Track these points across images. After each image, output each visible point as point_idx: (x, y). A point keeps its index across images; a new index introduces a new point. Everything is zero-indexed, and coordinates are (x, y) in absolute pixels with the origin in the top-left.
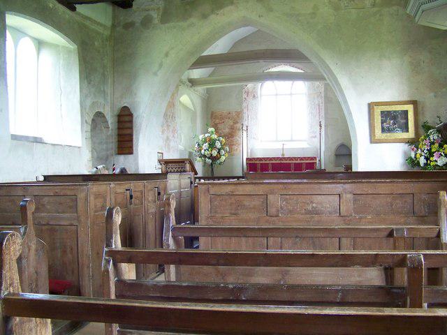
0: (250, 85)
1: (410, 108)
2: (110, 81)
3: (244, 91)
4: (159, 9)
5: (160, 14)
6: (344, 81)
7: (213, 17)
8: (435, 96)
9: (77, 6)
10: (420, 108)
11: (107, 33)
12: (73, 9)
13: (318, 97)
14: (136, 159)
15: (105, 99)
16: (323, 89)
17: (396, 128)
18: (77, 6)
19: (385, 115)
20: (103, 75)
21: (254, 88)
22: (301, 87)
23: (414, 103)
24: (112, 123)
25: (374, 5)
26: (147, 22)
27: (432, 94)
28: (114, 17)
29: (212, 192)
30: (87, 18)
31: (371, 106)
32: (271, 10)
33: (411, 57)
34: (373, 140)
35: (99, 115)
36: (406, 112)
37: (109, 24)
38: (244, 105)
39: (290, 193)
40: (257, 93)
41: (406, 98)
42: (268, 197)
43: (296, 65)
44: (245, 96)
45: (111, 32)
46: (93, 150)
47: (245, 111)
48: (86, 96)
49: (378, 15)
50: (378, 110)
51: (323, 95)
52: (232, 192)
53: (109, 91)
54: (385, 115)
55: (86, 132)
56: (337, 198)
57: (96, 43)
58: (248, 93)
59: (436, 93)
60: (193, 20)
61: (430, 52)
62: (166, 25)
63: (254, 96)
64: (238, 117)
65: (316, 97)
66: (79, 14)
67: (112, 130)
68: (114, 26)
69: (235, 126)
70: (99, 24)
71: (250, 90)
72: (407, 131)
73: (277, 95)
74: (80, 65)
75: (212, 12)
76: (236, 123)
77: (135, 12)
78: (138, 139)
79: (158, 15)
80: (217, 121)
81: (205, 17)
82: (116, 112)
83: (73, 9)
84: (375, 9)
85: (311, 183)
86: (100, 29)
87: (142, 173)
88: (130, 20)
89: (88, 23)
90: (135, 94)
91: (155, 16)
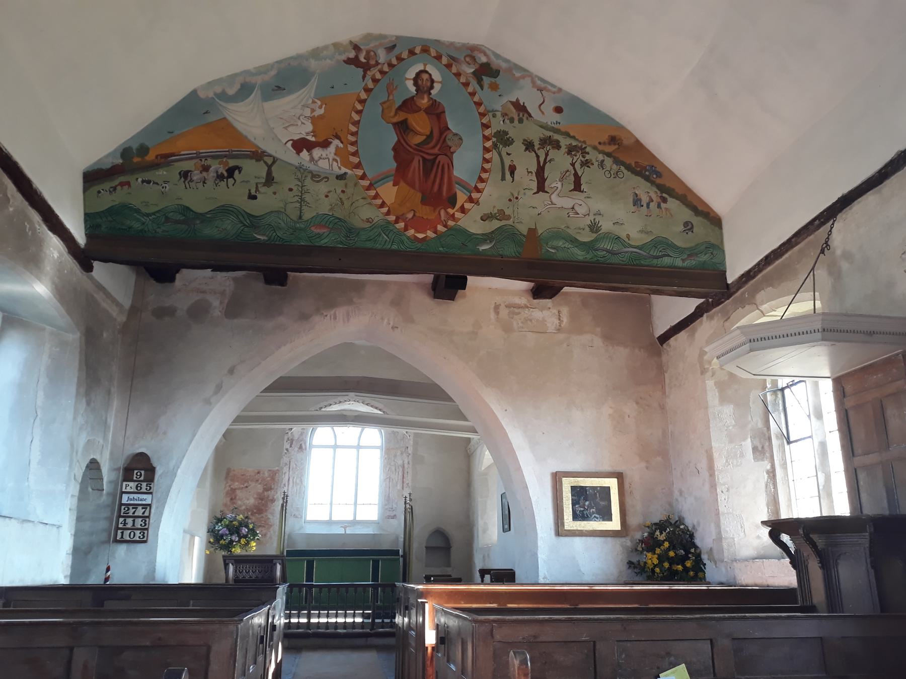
0: (296, 429)
1: (612, 483)
2: (115, 404)
3: (286, 437)
4: (223, 293)
5: (226, 301)
6: (516, 437)
7: (316, 318)
8: (647, 468)
9: (96, 264)
10: (627, 485)
11: (122, 318)
12: (87, 267)
13: (402, 454)
14: (153, 552)
15: (105, 437)
16: (411, 442)
17: (593, 513)
18: (96, 264)
19: (579, 493)
20: (109, 392)
21: (302, 434)
22: (373, 435)
23: (619, 476)
24: (110, 482)
25: (559, 330)
26: (198, 312)
27: (643, 465)
28: (139, 294)
29: (498, 637)
30: (100, 288)
31: (557, 478)
32: (409, 320)
33: (611, 407)
34: (560, 530)
35: (94, 466)
36: (607, 490)
37: (127, 303)
38: (285, 459)
39: (633, 637)
40: (305, 443)
41: (607, 468)
42: (598, 647)
43: (368, 400)
44: (287, 445)
45: (128, 319)
46: (77, 535)
47: (286, 469)
48: (81, 429)
49: (565, 345)
50: (567, 484)
51: (410, 450)
52: (535, 637)
53: (111, 422)
54: (579, 493)
55: (72, 496)
56: (707, 646)
57: (105, 335)
58: (291, 441)
59: (647, 462)
60: (282, 319)
61: (637, 403)
62: (235, 321)
63: (301, 447)
64: (273, 479)
65: (399, 453)
66: (92, 279)
67: (108, 494)
68: (134, 311)
69: (266, 493)
70: (114, 301)
71: (296, 437)
72: (610, 519)
73: (335, 447)
74: (80, 369)
75: (318, 311)
76: (268, 488)
77: (179, 290)
78: (161, 514)
79: (221, 303)
80: (236, 485)
81: (304, 317)
82: (121, 463)
83: (87, 267)
84: (561, 336)
85: (647, 619)
86: (114, 311)
87: (172, 580)
88: (167, 305)
89: (99, 297)
90: (165, 433)
91: (216, 303)
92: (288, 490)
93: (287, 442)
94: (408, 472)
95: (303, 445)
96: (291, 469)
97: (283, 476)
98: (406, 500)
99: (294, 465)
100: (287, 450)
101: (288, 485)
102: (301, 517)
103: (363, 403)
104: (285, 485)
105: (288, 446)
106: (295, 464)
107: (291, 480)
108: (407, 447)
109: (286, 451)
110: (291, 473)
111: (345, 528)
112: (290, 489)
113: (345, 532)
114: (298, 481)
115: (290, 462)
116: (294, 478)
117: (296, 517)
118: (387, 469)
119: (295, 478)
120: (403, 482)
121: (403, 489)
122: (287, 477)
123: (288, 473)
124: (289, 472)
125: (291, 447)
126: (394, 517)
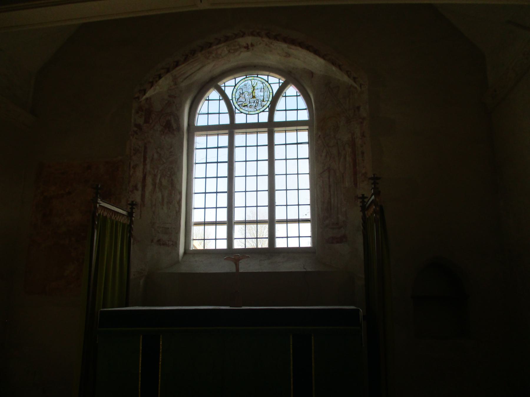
92: (143, 196)
93: (137, 113)
94: (363, 153)
95: (173, 121)
96: (148, 160)
97: (131, 172)
98: (363, 202)
99: (156, 156)
100: (138, 126)
101: (144, 186)
102: (176, 244)
103: (268, 36)
104: (136, 187)
105: (141, 121)
106: (157, 152)
107: (149, 180)
108: (358, 108)
109: (136, 129)
110: (148, 167)
111: (236, 262)
112: (147, 194)
113: (237, 269)
114: (165, 182)
115: (146, 148)
116: (155, 176)
117: (164, 244)
118: (324, 154)
119: (159, 177)
120: (355, 173)
121: (356, 184)
122: (139, 174)
123: (141, 167)
124: (145, 164)
125: (146, 121)
126: (342, 239)
